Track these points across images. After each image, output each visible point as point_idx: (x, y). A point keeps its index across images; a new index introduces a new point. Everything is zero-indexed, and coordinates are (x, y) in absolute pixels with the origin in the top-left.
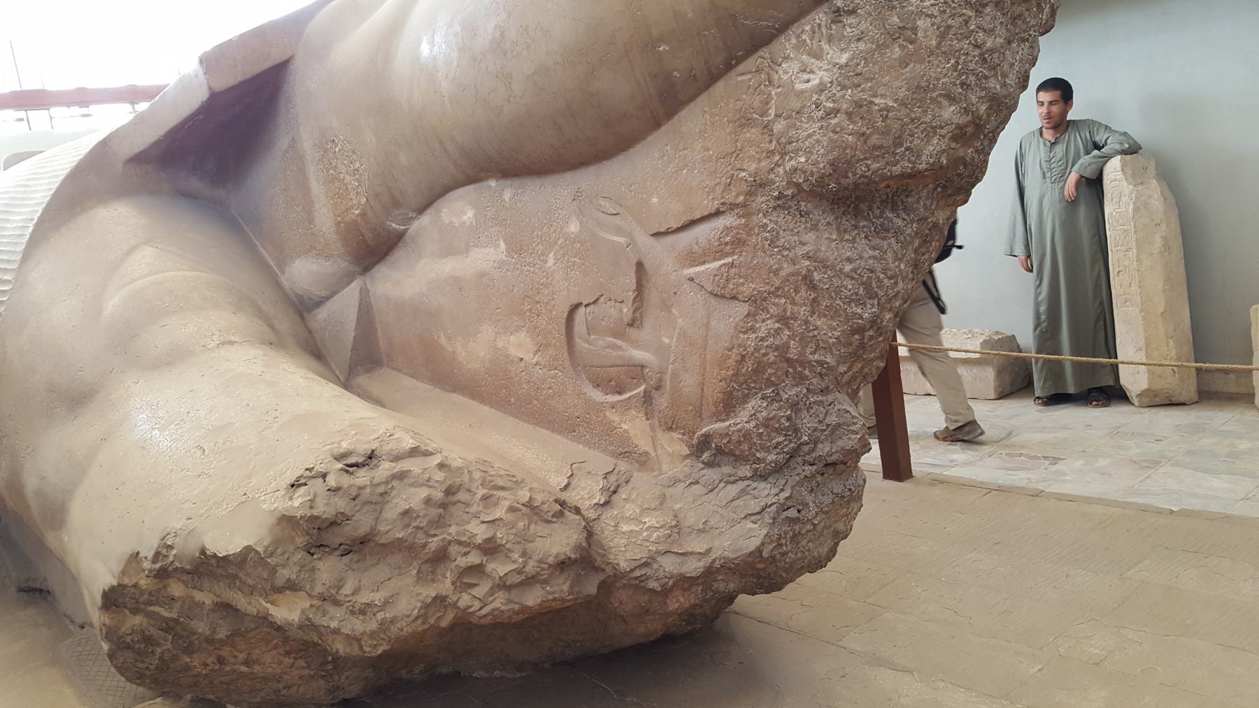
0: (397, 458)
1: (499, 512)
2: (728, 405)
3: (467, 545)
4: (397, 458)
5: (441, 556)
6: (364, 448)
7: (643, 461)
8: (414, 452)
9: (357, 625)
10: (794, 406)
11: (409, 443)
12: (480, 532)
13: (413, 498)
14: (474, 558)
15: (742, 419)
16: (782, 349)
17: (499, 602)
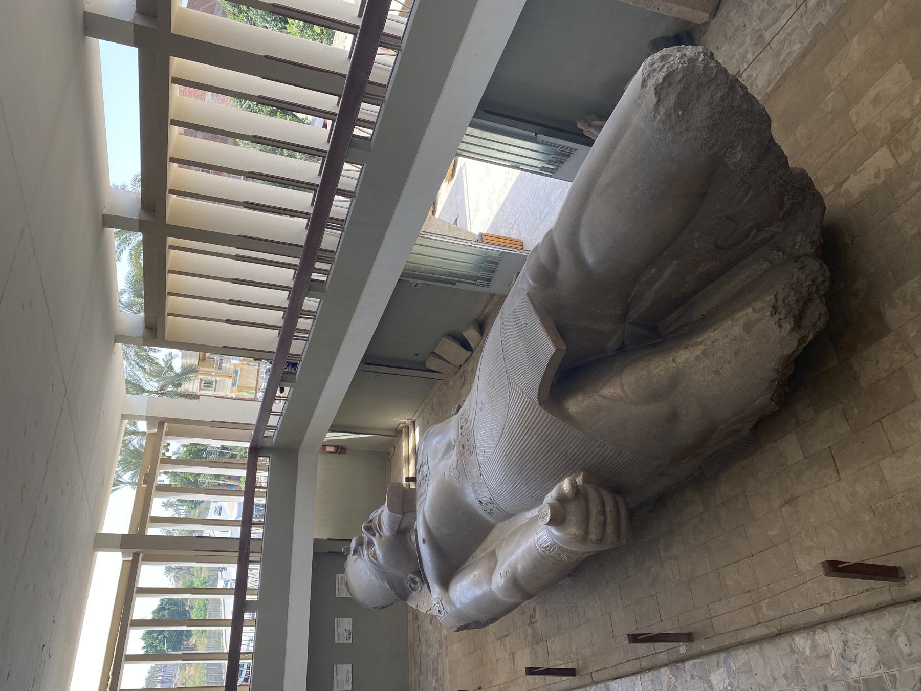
0: (776, 301)
1: (803, 277)
2: (782, 206)
3: (809, 286)
4: (776, 301)
5: (809, 294)
6: (771, 309)
7: (772, 237)
8: (775, 296)
9: (823, 319)
10: (793, 187)
11: (772, 297)
12: (809, 282)
13: (792, 298)
14: (814, 288)
15: (788, 203)
16: (780, 186)
17: (827, 284)
